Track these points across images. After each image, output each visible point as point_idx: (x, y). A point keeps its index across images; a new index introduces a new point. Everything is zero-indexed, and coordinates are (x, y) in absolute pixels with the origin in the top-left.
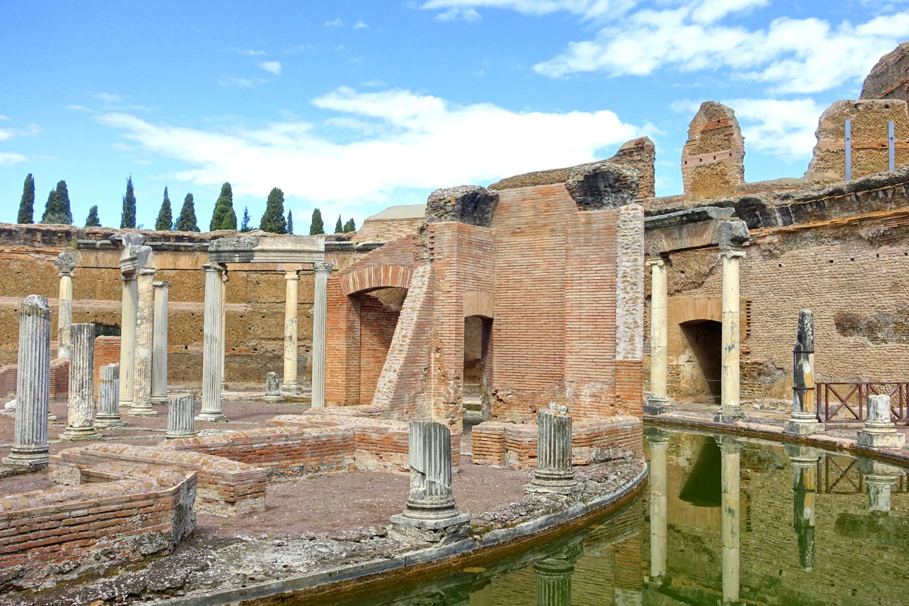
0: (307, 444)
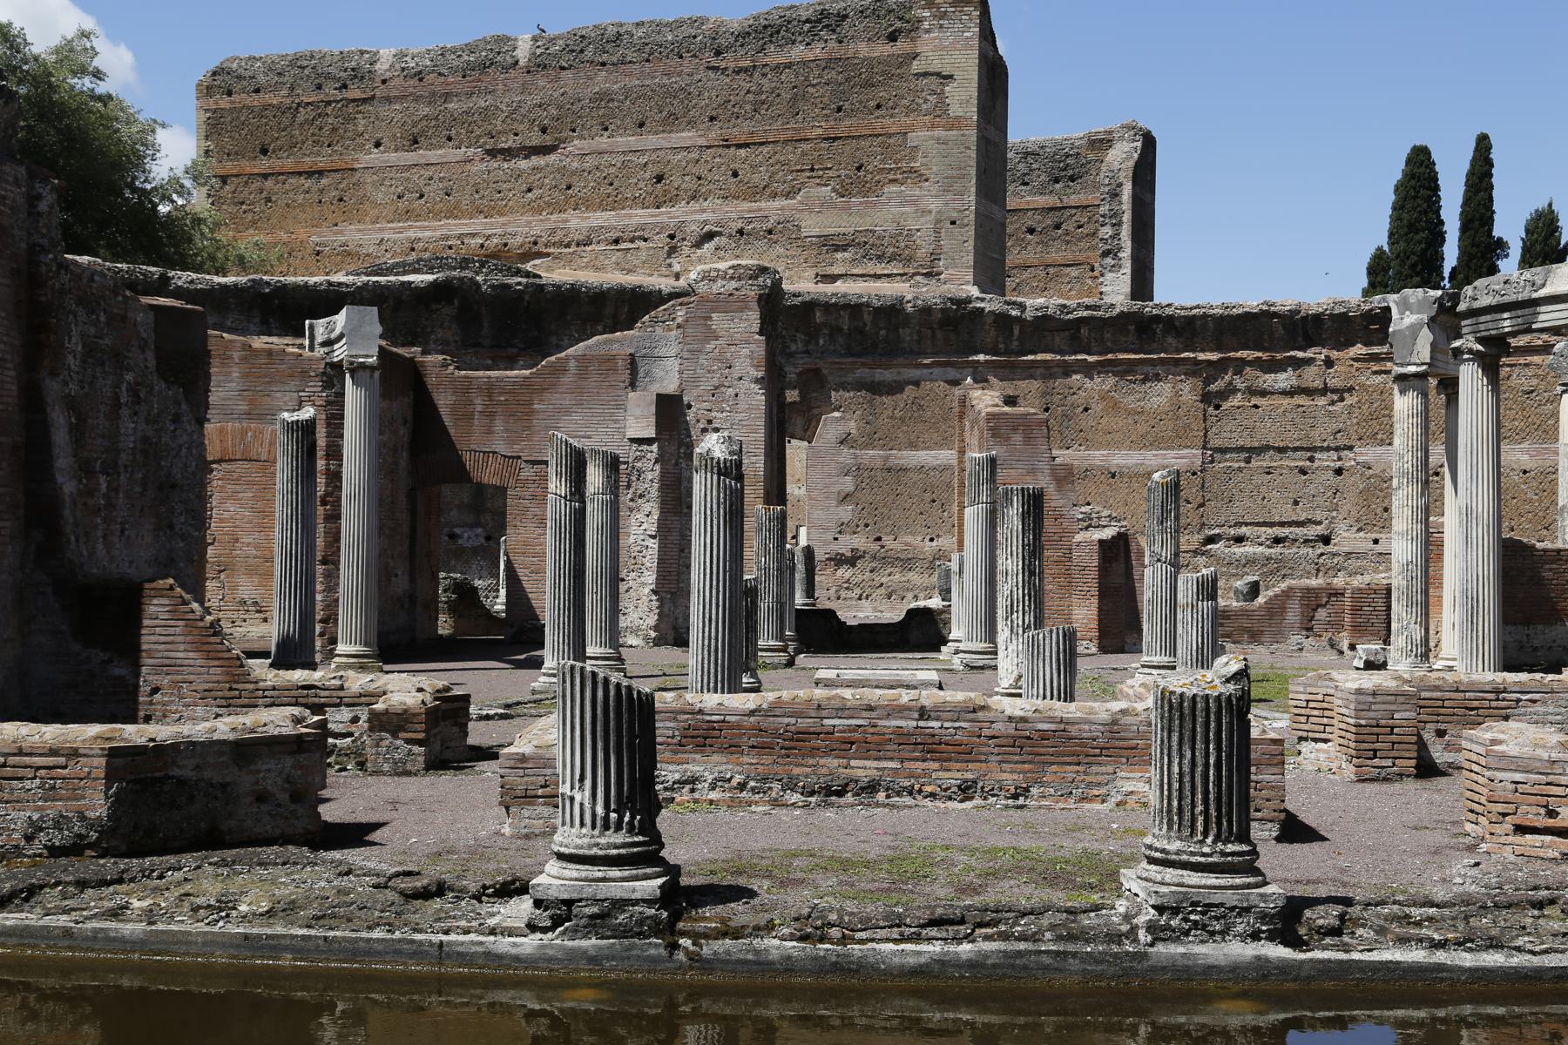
0: (986, 732)
